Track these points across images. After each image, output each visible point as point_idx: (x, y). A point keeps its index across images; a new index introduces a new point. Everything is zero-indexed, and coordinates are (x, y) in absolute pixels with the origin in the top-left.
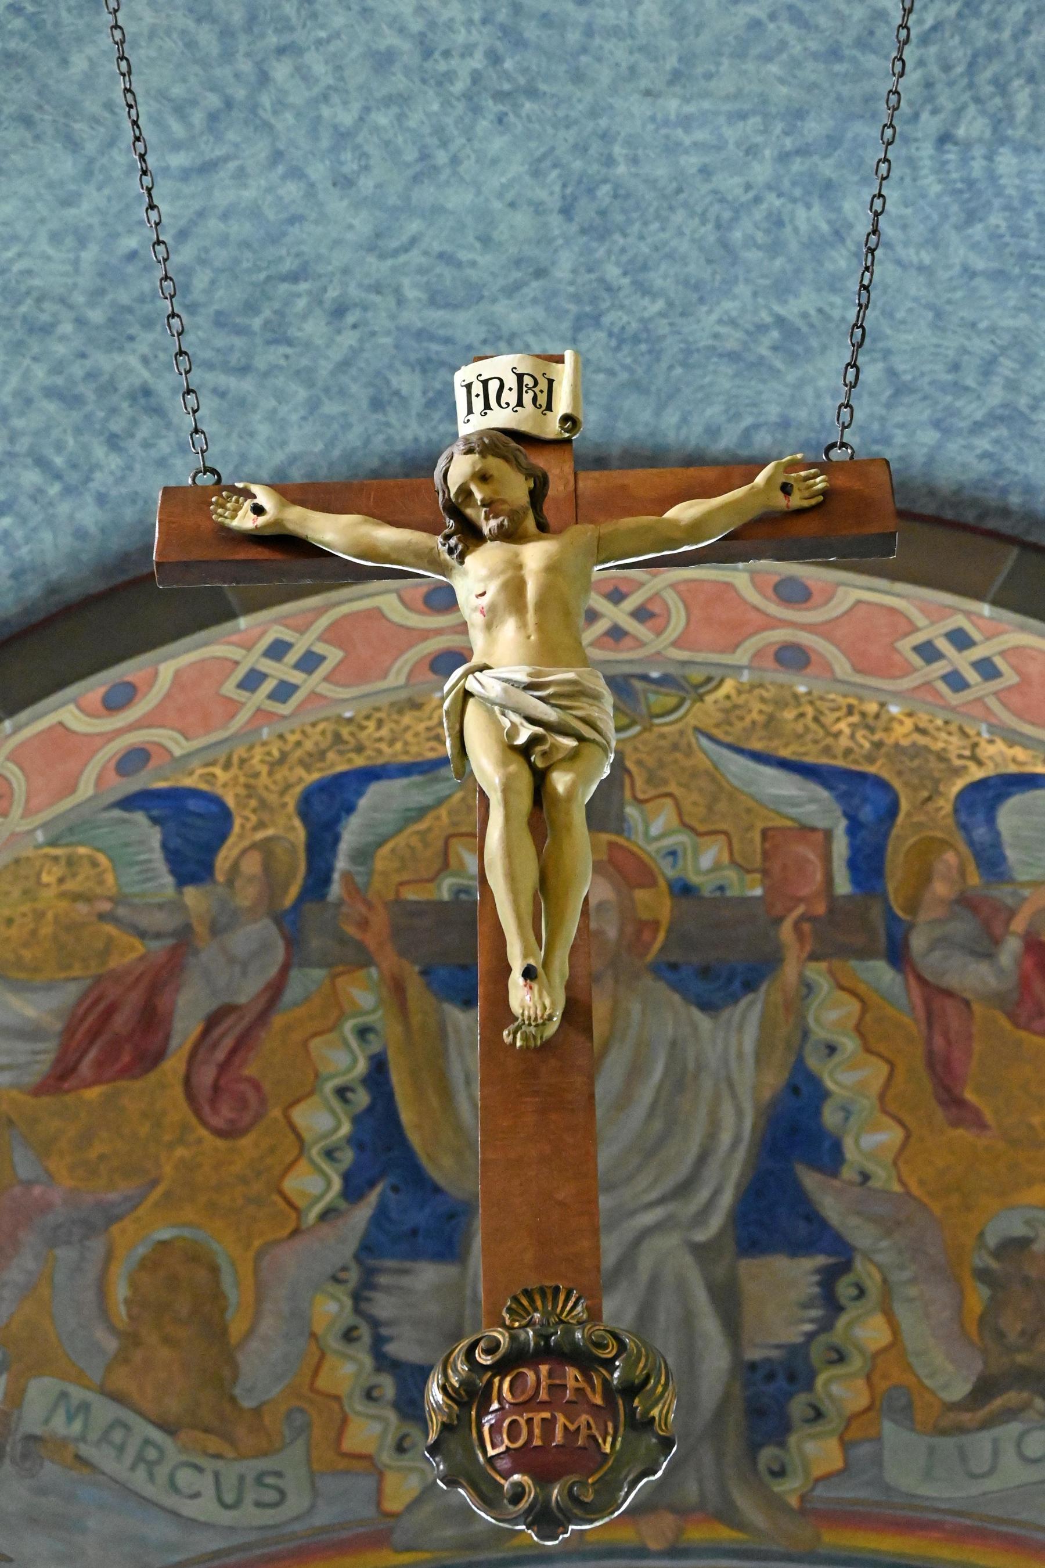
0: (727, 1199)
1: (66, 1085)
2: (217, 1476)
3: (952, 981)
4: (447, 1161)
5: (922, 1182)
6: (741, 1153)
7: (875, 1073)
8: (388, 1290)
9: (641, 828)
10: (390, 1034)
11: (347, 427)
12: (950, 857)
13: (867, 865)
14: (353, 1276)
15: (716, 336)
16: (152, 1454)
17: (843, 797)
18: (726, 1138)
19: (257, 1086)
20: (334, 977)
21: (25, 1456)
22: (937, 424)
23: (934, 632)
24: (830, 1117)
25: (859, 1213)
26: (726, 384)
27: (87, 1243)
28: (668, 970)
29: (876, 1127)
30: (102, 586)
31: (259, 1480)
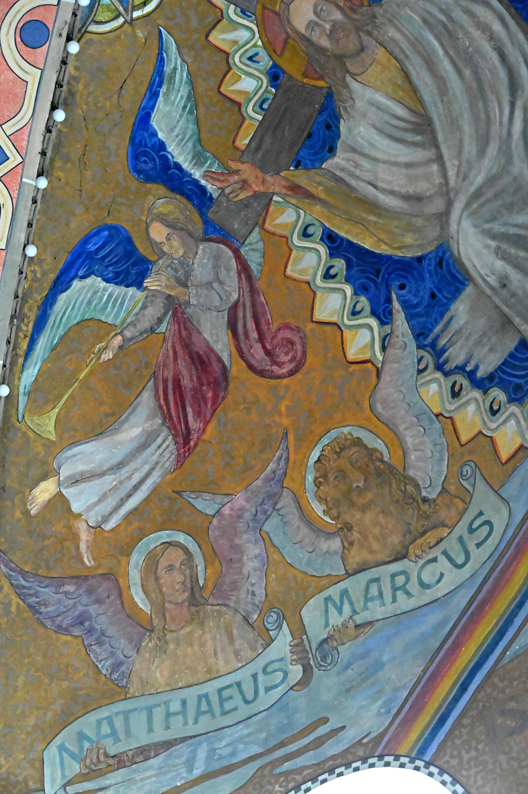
1: (192, 444)
2: (445, 553)
4: (409, 239)
8: (451, 343)
10: (317, 216)
14: (428, 359)
16: (400, 580)
19: (287, 327)
20: (263, 228)
21: (324, 658)
27: (278, 506)
31: (471, 530)
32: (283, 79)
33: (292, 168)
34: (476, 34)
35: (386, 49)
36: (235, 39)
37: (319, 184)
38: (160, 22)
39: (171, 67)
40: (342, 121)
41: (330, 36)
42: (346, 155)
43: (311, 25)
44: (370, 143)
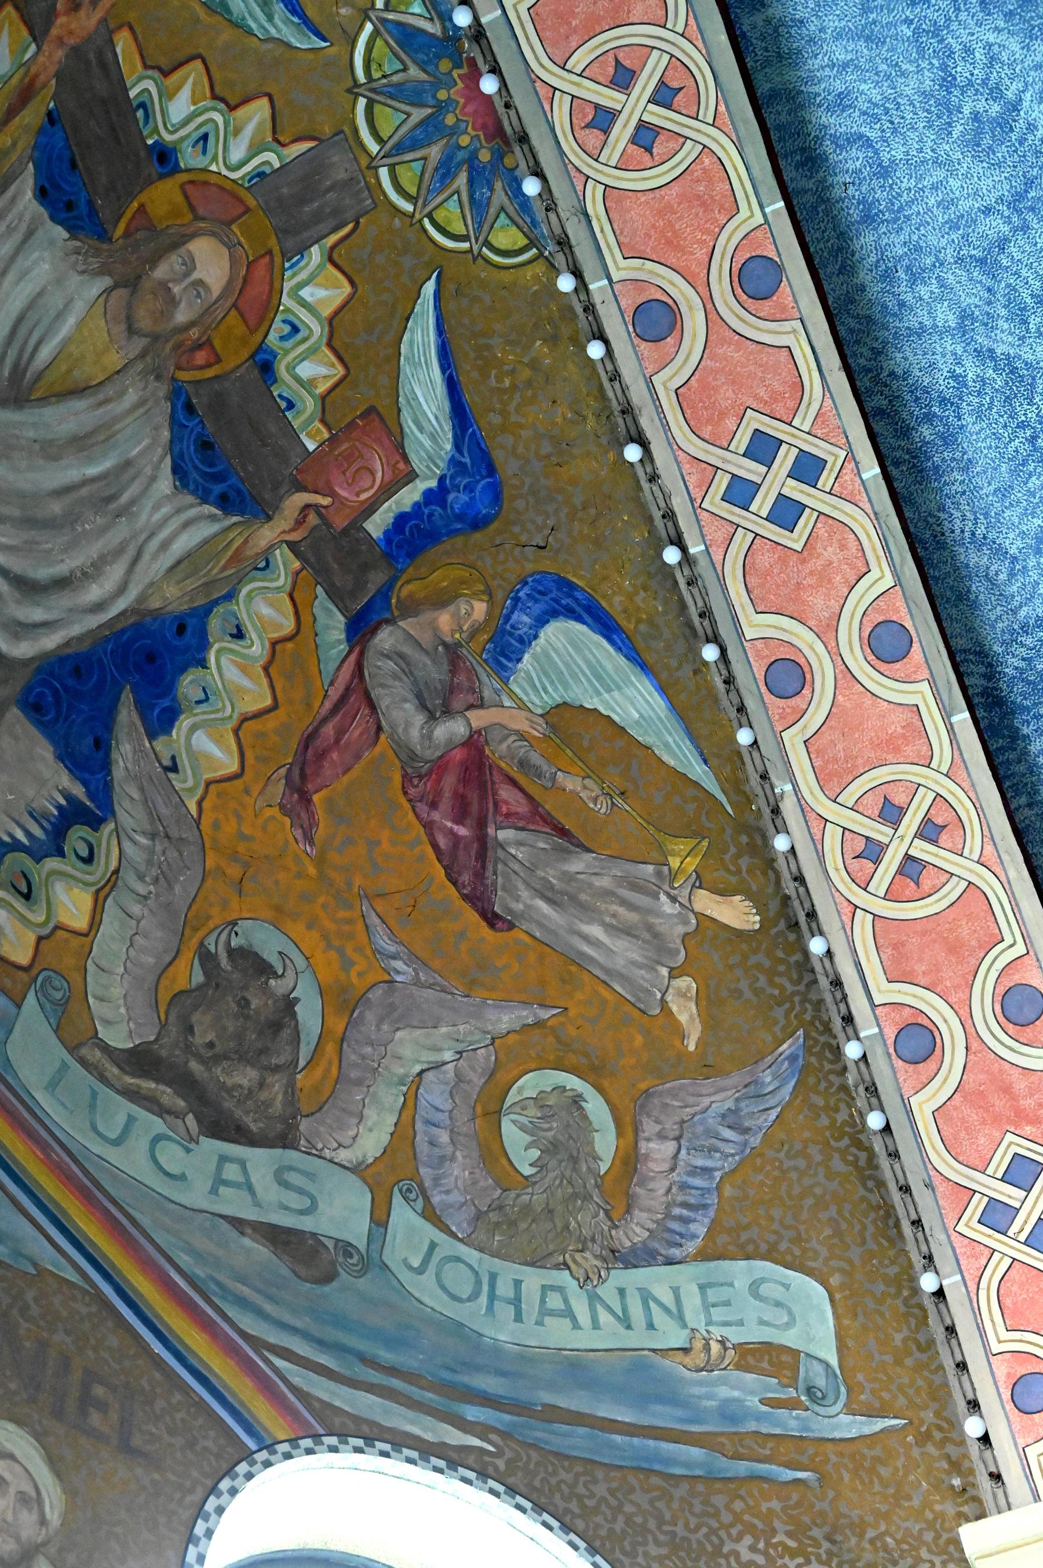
0: (50, 642)
3: (384, 699)
5: (216, 825)
6: (94, 621)
7: (256, 695)
9: (303, 276)
13: (413, 535)
15: (968, 51)
18: (94, 593)
22: (965, 316)
23: (796, 437)
24: (188, 685)
25: (142, 789)
26: (909, 87)
28: (183, 406)
29: (219, 741)
32: (155, 168)
33: (52, 104)
34: (93, 550)
35: (118, 372)
36: (240, 136)
37: (14, 144)
38: (333, 50)
39: (276, 17)
40: (65, 235)
41: (164, 286)
42: (27, 217)
43: (190, 265)
44: (28, 272)
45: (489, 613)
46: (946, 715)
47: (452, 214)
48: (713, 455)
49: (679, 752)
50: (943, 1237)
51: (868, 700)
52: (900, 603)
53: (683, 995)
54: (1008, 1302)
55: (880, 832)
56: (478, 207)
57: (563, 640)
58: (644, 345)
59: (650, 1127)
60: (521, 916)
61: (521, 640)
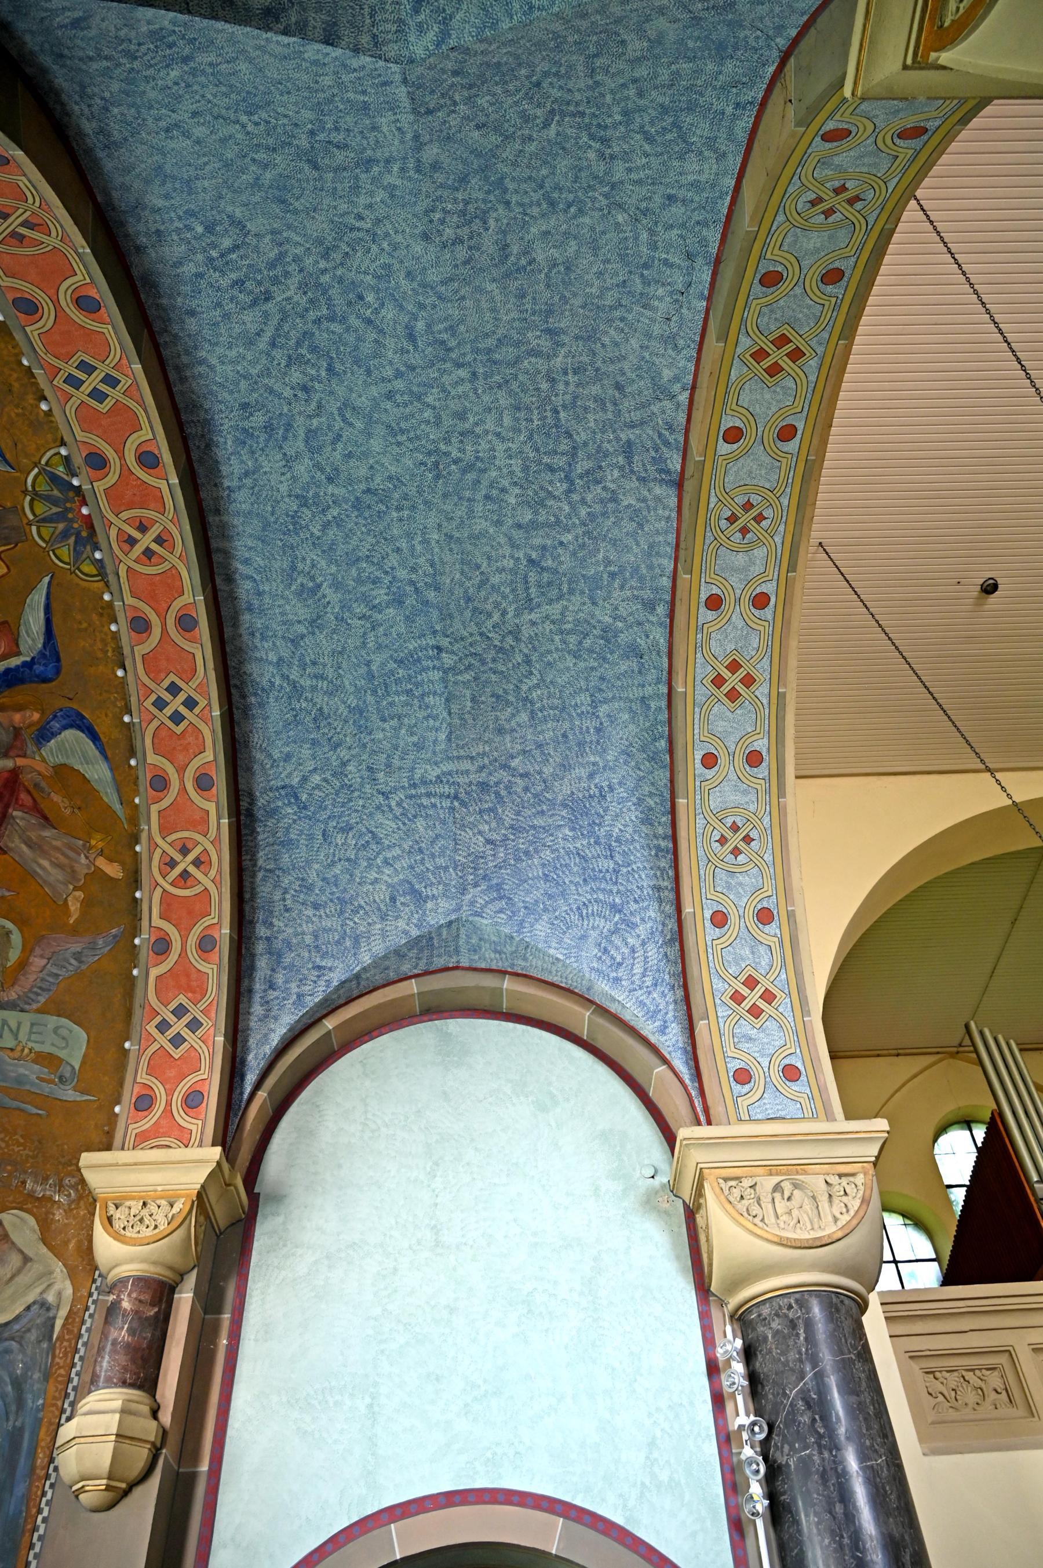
11: (231, 392)
12: (36, 716)
15: (304, 559)
17: (42, 654)
22: (281, 659)
26: (277, 565)
30: (135, 272)
45: (40, 719)
46: (219, 818)
47: (64, 552)
48: (152, 685)
49: (111, 797)
50: (139, 1029)
51: (189, 803)
52: (214, 768)
53: (76, 899)
54: (152, 1062)
55: (178, 857)
56: (78, 554)
57: (71, 735)
58: (133, 633)
59: (38, 951)
60: (11, 849)
61: (52, 734)
